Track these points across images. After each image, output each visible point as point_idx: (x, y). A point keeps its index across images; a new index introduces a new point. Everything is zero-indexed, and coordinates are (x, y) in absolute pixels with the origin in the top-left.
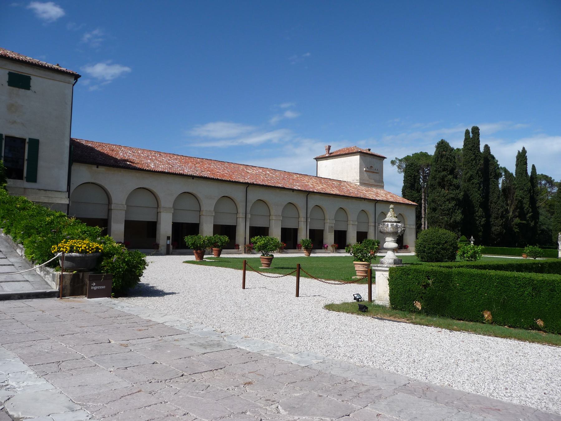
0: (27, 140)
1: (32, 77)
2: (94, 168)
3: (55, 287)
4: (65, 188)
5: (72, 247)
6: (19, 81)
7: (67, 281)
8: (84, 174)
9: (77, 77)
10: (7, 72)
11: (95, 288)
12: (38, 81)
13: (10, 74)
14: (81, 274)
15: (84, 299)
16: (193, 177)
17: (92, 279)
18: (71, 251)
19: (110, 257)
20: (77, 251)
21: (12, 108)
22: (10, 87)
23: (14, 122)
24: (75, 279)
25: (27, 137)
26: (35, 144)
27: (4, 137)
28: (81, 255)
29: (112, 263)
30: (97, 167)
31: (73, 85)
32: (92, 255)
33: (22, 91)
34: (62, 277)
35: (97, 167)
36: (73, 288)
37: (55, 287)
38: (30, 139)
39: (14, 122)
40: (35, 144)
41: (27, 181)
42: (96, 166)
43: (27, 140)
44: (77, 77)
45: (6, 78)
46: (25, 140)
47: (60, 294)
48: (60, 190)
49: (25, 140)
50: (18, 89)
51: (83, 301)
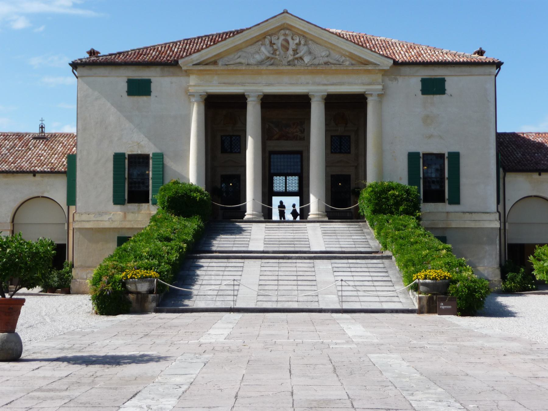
0: (446, 155)
1: (446, 78)
2: (535, 176)
3: (416, 307)
4: (493, 206)
5: (426, 276)
6: (433, 87)
7: (425, 302)
8: (521, 185)
9: (498, 65)
10: (420, 79)
11: (443, 307)
12: (454, 82)
14: (435, 297)
15: (436, 316)
17: (443, 300)
18: (425, 278)
19: (456, 283)
20: (430, 279)
21: (427, 120)
22: (425, 96)
23: (431, 136)
24: (430, 300)
25: (445, 150)
26: (455, 157)
27: (421, 155)
28: (432, 281)
29: (456, 288)
30: (540, 175)
31: (496, 76)
33: (437, 98)
34: (420, 299)
35: (540, 175)
36: (430, 307)
37: (416, 307)
38: (450, 154)
39: (431, 136)
40: (455, 157)
41: (450, 203)
42: (538, 173)
43: (446, 155)
44: (498, 65)
45: (419, 86)
46: (444, 155)
47: (420, 311)
48: (488, 211)
49: (444, 155)
50: (432, 96)
51: (435, 317)
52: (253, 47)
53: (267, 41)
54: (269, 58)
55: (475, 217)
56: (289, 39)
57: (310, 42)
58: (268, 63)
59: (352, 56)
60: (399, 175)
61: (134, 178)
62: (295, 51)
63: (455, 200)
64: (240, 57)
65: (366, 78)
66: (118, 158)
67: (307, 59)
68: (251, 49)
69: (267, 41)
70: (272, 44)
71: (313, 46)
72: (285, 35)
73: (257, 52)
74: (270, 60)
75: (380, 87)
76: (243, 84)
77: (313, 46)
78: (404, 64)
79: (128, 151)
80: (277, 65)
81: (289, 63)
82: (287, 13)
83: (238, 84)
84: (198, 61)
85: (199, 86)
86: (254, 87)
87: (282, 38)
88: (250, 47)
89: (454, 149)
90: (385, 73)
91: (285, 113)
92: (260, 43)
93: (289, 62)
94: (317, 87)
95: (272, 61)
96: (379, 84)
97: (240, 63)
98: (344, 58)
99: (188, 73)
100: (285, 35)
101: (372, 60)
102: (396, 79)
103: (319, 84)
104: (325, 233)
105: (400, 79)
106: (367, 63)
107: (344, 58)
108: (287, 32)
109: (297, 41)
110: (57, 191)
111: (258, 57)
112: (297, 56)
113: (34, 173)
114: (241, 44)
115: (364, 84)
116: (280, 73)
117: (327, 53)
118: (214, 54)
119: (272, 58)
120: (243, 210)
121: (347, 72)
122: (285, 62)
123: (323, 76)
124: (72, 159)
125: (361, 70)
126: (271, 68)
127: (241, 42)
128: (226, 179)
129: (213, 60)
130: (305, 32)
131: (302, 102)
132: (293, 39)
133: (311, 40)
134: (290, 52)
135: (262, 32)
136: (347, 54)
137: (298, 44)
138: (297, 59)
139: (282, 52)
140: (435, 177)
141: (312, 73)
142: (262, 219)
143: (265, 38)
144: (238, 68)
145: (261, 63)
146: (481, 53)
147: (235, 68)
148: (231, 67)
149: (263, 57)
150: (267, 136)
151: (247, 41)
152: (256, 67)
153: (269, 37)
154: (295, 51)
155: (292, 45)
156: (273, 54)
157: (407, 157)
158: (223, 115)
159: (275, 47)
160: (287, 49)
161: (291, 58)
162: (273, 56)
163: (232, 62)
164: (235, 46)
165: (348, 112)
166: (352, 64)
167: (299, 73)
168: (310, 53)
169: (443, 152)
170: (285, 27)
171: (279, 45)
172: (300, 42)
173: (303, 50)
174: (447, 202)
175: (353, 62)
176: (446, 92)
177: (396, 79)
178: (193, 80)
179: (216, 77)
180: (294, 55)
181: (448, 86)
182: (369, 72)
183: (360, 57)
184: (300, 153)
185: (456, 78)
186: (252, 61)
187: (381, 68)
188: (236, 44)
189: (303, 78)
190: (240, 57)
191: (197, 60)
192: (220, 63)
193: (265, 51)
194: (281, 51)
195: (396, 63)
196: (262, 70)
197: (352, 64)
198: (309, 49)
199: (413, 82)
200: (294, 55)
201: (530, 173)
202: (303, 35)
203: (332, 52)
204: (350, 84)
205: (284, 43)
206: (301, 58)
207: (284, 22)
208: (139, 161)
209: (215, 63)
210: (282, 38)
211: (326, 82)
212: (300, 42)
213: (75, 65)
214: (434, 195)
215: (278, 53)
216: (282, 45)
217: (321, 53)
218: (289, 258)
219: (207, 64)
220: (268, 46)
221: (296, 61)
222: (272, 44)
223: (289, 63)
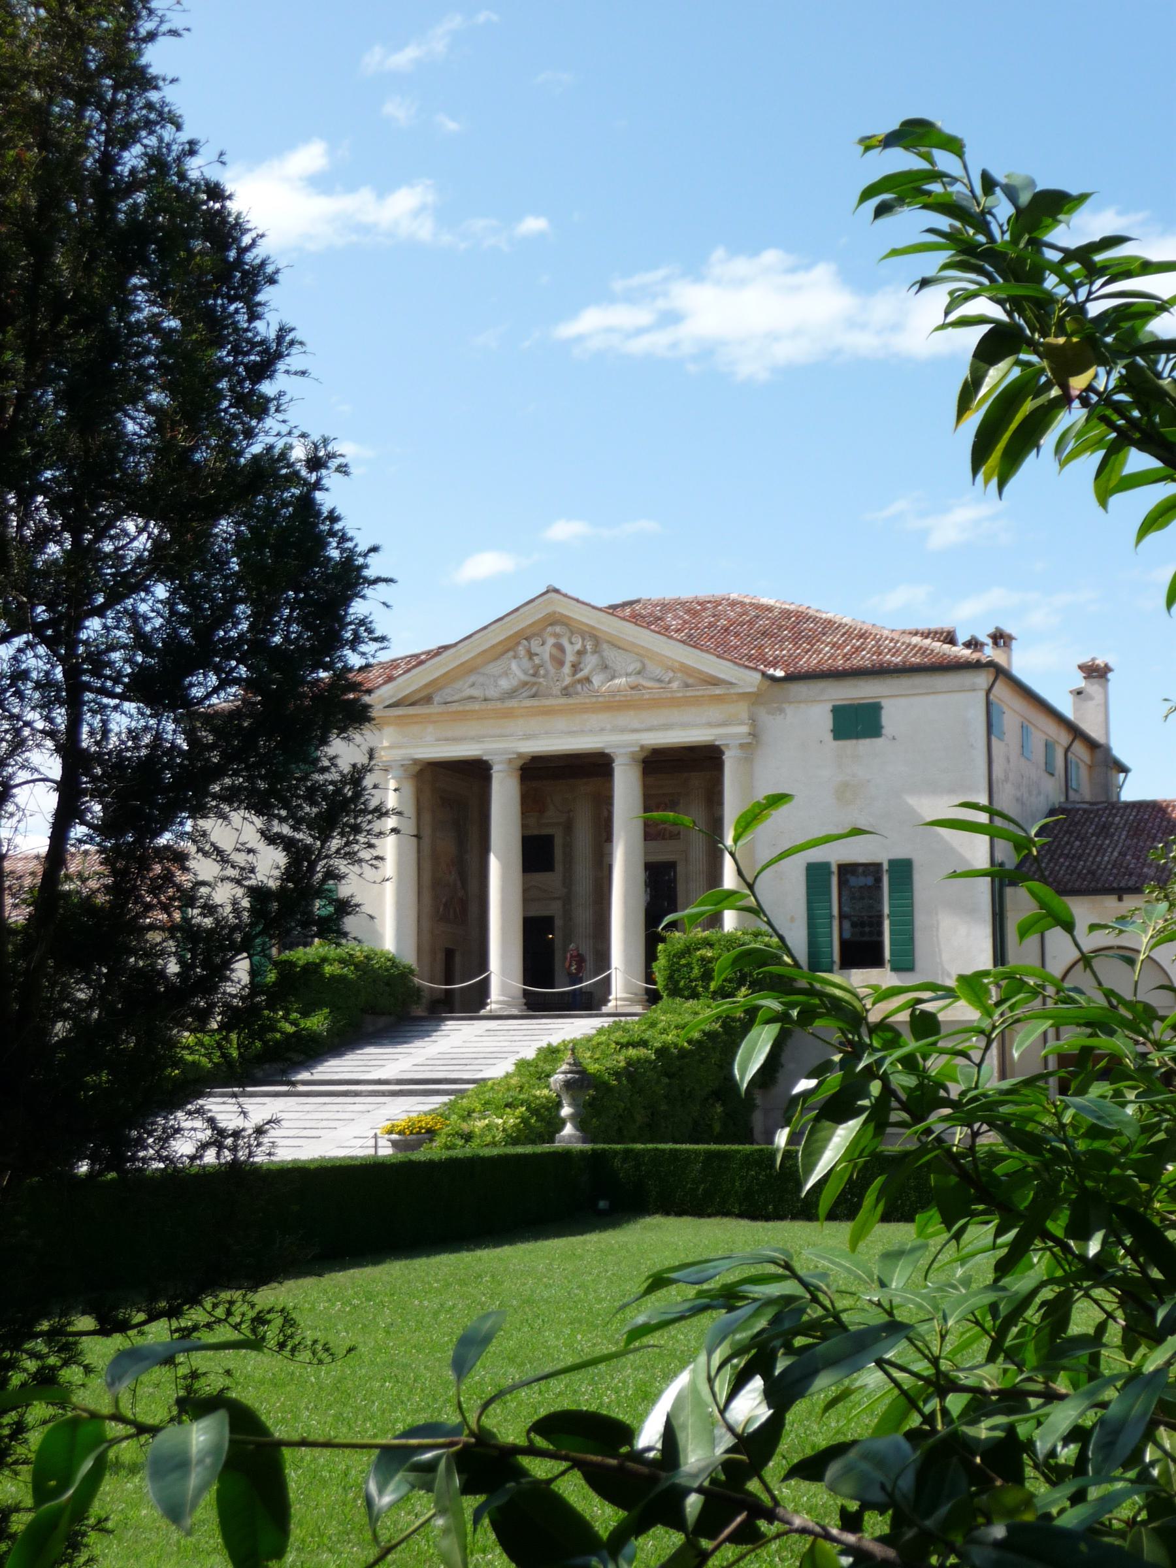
0: (886, 867)
1: (883, 704)
6: (857, 723)
10: (829, 706)
12: (901, 707)
13: (837, 711)
27: (834, 869)
30: (1120, 899)
32: (412, 1137)
33: (865, 745)
35: (1120, 899)
38: (892, 863)
43: (886, 867)
45: (827, 722)
49: (878, 866)
50: (854, 742)
52: (499, 662)
53: (521, 650)
54: (525, 684)
56: (565, 642)
57: (605, 646)
58: (525, 694)
59: (686, 670)
62: (576, 667)
64: (473, 685)
65: (715, 713)
68: (494, 668)
69: (521, 650)
70: (531, 655)
71: (610, 654)
72: (556, 635)
73: (506, 674)
74: (531, 688)
75: (744, 729)
76: (478, 739)
80: (548, 696)
81: (566, 692)
82: (557, 591)
83: (473, 739)
84: (395, 700)
85: (400, 747)
86: (505, 743)
88: (491, 666)
89: (900, 853)
90: (755, 699)
92: (511, 654)
93: (566, 688)
94: (622, 737)
95: (534, 689)
96: (742, 724)
97: (471, 698)
98: (671, 674)
100: (556, 635)
101: (722, 676)
102: (781, 711)
103: (623, 730)
105: (790, 710)
106: (715, 682)
107: (671, 674)
108: (558, 629)
109: (578, 647)
111: (505, 684)
112: (579, 676)
114: (473, 658)
115: (710, 725)
116: (548, 712)
117: (638, 666)
118: (423, 682)
119: (534, 684)
120: (483, 989)
121: (675, 703)
122: (556, 690)
123: (632, 713)
125: (703, 696)
126: (528, 703)
127: (472, 655)
129: (422, 694)
130: (593, 628)
131: (594, 768)
132: (572, 643)
133: (608, 642)
134: (567, 669)
135: (512, 632)
136: (676, 664)
137: (581, 653)
138: (579, 681)
139: (552, 671)
142: (515, 1012)
143: (518, 643)
144: (467, 708)
145: (511, 694)
147: (461, 708)
148: (454, 707)
149: (515, 683)
151: (484, 651)
152: (499, 705)
153: (525, 642)
154: (576, 667)
155: (570, 657)
156: (534, 675)
157: (804, 872)
159: (537, 660)
160: (561, 663)
161: (568, 681)
162: (534, 679)
163: (455, 698)
164: (462, 664)
166: (687, 686)
168: (606, 667)
169: (878, 861)
170: (554, 620)
171: (547, 656)
172: (584, 646)
173: (591, 661)
174: (888, 966)
175: (690, 681)
176: (884, 731)
177: (781, 711)
179: (431, 728)
180: (574, 673)
181: (889, 718)
182: (719, 699)
183: (701, 672)
185: (903, 701)
186: (492, 693)
187: (741, 691)
188: (463, 660)
190: (473, 685)
191: (391, 697)
192: (437, 699)
193: (516, 670)
196: (513, 708)
197: (687, 686)
198: (602, 657)
199: (814, 712)
200: (574, 673)
201: (1098, 897)
203: (646, 661)
204: (684, 726)
205: (555, 651)
206: (588, 680)
207: (550, 609)
209: (428, 700)
210: (551, 641)
211: (636, 725)
212: (584, 646)
214: (862, 951)
215: (542, 672)
216: (552, 656)
218: (357, 1094)
219: (413, 704)
220: (526, 662)
221: (579, 687)
222: (531, 655)
223: (566, 692)
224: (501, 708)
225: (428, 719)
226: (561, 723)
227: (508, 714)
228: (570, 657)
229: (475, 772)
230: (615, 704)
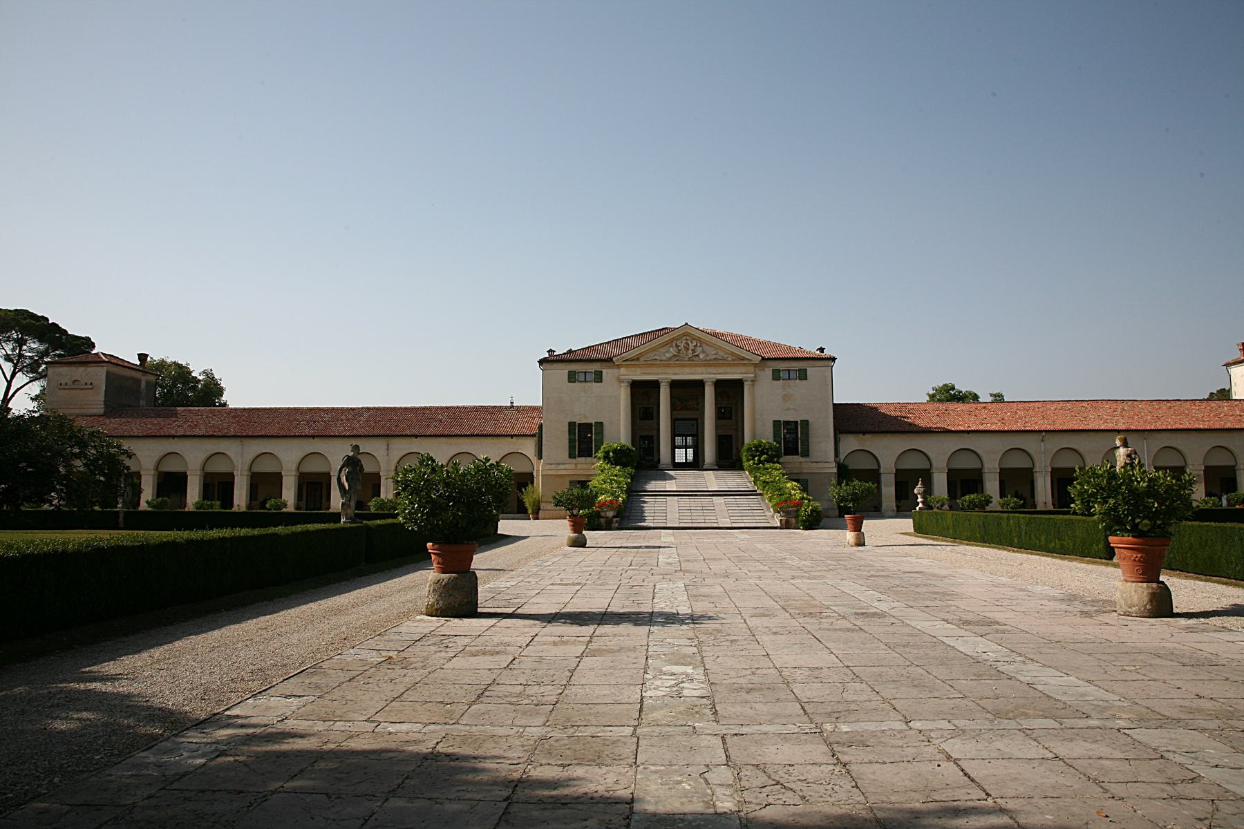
4: (832, 459)
8: (851, 443)
9: (834, 359)
16: (968, 432)
21: (786, 398)
25: (798, 419)
26: (805, 423)
36: (786, 525)
40: (805, 423)
44: (834, 359)
55: (820, 465)
59: (733, 354)
60: (767, 437)
61: (584, 439)
62: (693, 351)
63: (806, 454)
65: (743, 369)
66: (572, 425)
67: (701, 356)
68: (663, 350)
77: (706, 348)
78: (769, 359)
79: (578, 420)
86: (665, 376)
87: (684, 340)
90: (756, 365)
91: (688, 392)
94: (708, 375)
99: (619, 367)
104: (716, 478)
106: (744, 359)
110: (528, 447)
113: (512, 436)
116: (684, 366)
121: (730, 365)
124: (541, 427)
128: (643, 438)
140: (792, 438)
141: (705, 365)
145: (670, 359)
146: (822, 350)
150: (673, 407)
154: (693, 351)
155: (691, 346)
158: (643, 394)
165: (730, 392)
167: (696, 365)
173: (699, 350)
178: (623, 370)
184: (696, 419)
189: (699, 370)
193: (673, 351)
194: (683, 351)
195: (763, 358)
202: (699, 340)
208: (585, 427)
209: (638, 359)
213: (541, 362)
214: (791, 450)
217: (711, 352)
224: (666, 364)
225: (639, 366)
226: (687, 370)
227: (668, 366)
228: (691, 346)
229: (655, 385)
230: (707, 364)
